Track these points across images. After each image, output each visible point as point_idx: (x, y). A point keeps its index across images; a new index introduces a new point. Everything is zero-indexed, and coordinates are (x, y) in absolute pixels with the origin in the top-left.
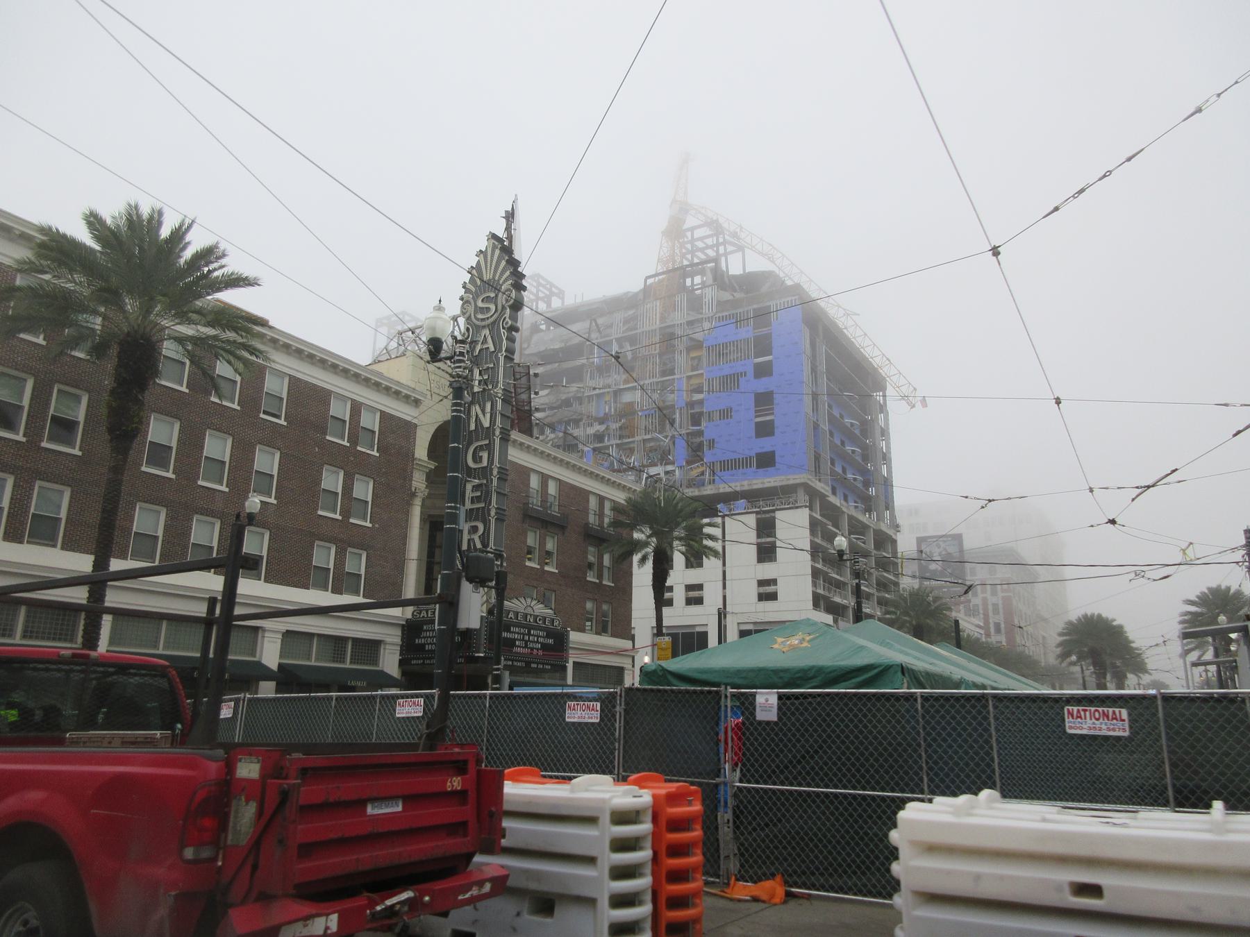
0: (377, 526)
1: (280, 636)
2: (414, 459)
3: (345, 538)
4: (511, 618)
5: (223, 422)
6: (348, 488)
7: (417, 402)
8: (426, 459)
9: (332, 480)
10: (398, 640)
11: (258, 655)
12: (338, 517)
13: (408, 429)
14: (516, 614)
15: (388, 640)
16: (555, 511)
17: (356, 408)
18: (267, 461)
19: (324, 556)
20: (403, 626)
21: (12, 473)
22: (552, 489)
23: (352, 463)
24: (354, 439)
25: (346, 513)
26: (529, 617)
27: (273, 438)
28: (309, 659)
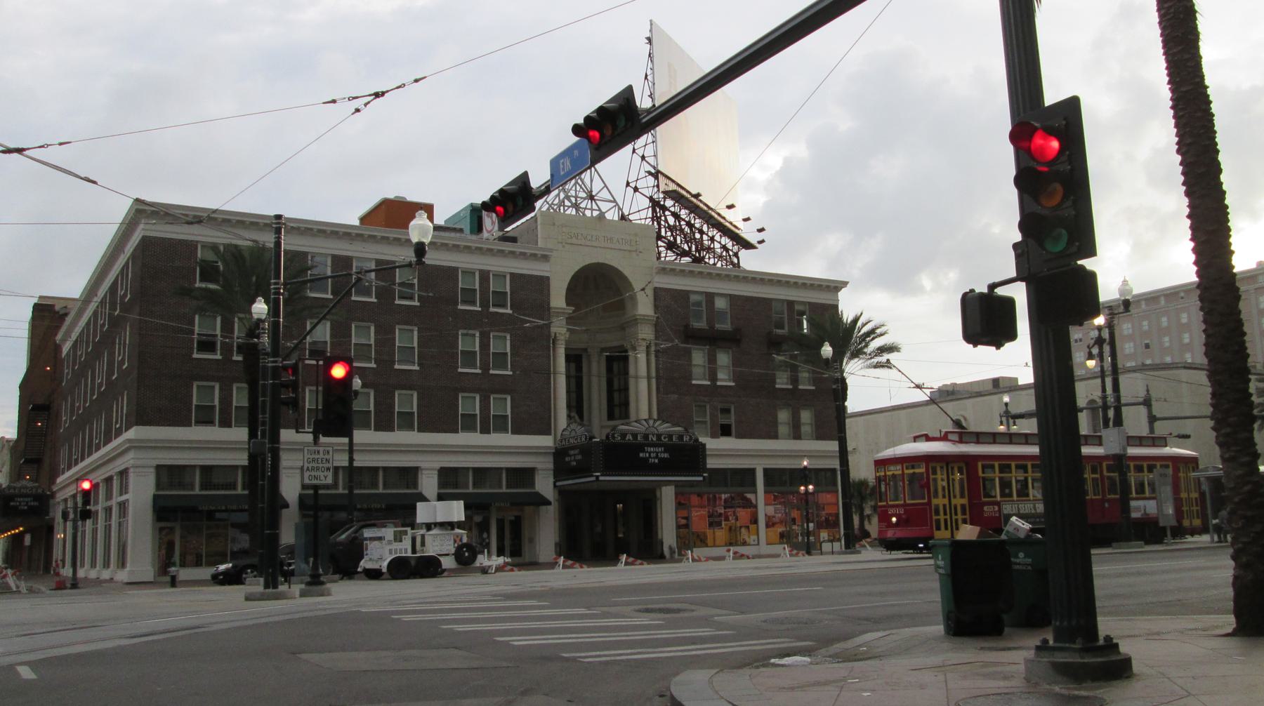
0: (518, 372)
1: (436, 472)
2: (549, 308)
3: (487, 387)
4: (629, 440)
5: (365, 313)
6: (485, 346)
7: (545, 258)
8: (564, 305)
9: (468, 342)
10: (551, 466)
11: (420, 488)
12: (478, 371)
13: (542, 284)
14: (635, 436)
15: (538, 466)
16: (726, 326)
17: (485, 276)
18: (407, 338)
19: (469, 404)
20: (554, 453)
21: (217, 381)
22: (720, 304)
23: (486, 323)
24: (485, 304)
25: (485, 368)
26: (650, 436)
27: (408, 316)
28: (500, 487)
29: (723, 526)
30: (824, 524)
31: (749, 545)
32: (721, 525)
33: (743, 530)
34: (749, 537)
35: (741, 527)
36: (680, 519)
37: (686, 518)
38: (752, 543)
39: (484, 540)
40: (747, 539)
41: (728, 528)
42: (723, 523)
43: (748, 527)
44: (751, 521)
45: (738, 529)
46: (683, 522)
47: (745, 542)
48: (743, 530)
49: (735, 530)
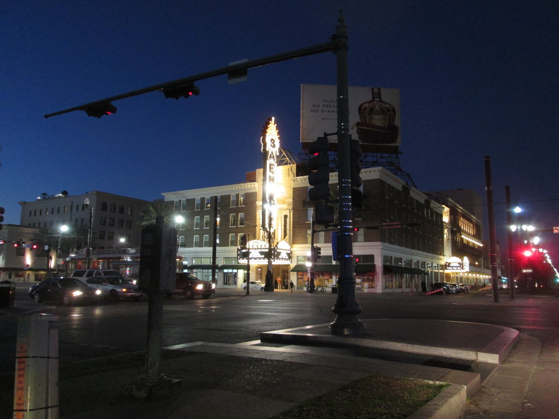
29: (317, 279)
30: (366, 280)
31: (328, 287)
32: (316, 278)
33: (326, 281)
34: (328, 284)
35: (325, 280)
36: (299, 276)
37: (302, 275)
38: (329, 286)
39: (235, 280)
40: (328, 285)
41: (319, 280)
42: (317, 278)
43: (328, 280)
44: (329, 277)
45: (324, 280)
46: (301, 277)
47: (327, 286)
48: (326, 281)
49: (322, 281)
